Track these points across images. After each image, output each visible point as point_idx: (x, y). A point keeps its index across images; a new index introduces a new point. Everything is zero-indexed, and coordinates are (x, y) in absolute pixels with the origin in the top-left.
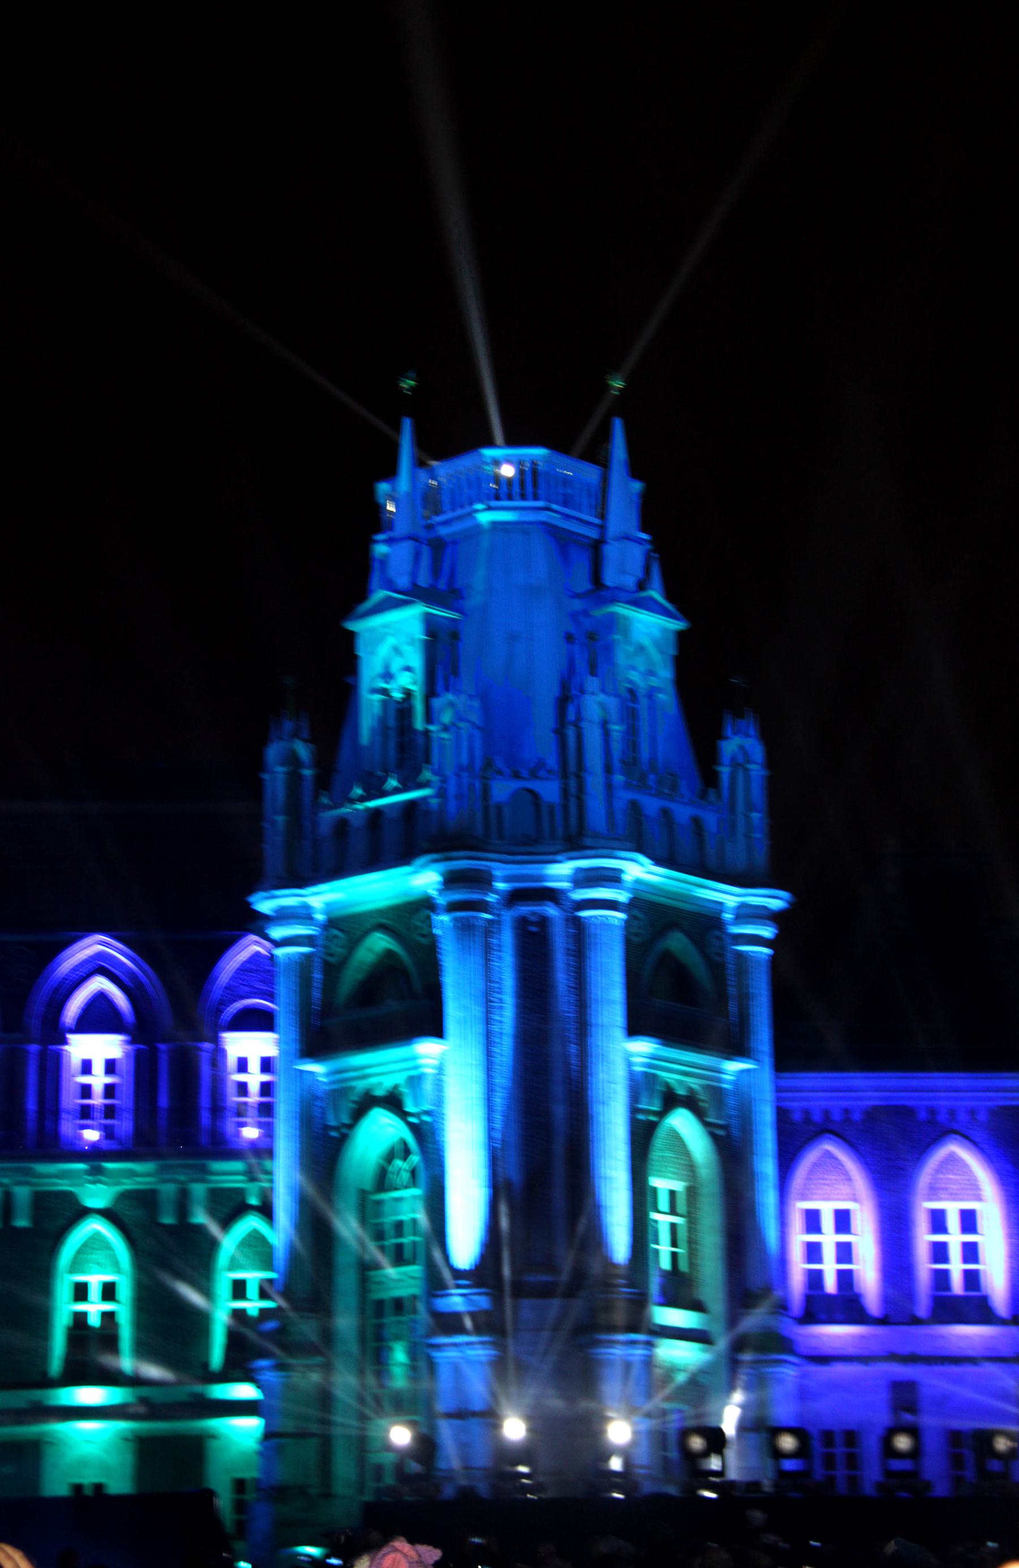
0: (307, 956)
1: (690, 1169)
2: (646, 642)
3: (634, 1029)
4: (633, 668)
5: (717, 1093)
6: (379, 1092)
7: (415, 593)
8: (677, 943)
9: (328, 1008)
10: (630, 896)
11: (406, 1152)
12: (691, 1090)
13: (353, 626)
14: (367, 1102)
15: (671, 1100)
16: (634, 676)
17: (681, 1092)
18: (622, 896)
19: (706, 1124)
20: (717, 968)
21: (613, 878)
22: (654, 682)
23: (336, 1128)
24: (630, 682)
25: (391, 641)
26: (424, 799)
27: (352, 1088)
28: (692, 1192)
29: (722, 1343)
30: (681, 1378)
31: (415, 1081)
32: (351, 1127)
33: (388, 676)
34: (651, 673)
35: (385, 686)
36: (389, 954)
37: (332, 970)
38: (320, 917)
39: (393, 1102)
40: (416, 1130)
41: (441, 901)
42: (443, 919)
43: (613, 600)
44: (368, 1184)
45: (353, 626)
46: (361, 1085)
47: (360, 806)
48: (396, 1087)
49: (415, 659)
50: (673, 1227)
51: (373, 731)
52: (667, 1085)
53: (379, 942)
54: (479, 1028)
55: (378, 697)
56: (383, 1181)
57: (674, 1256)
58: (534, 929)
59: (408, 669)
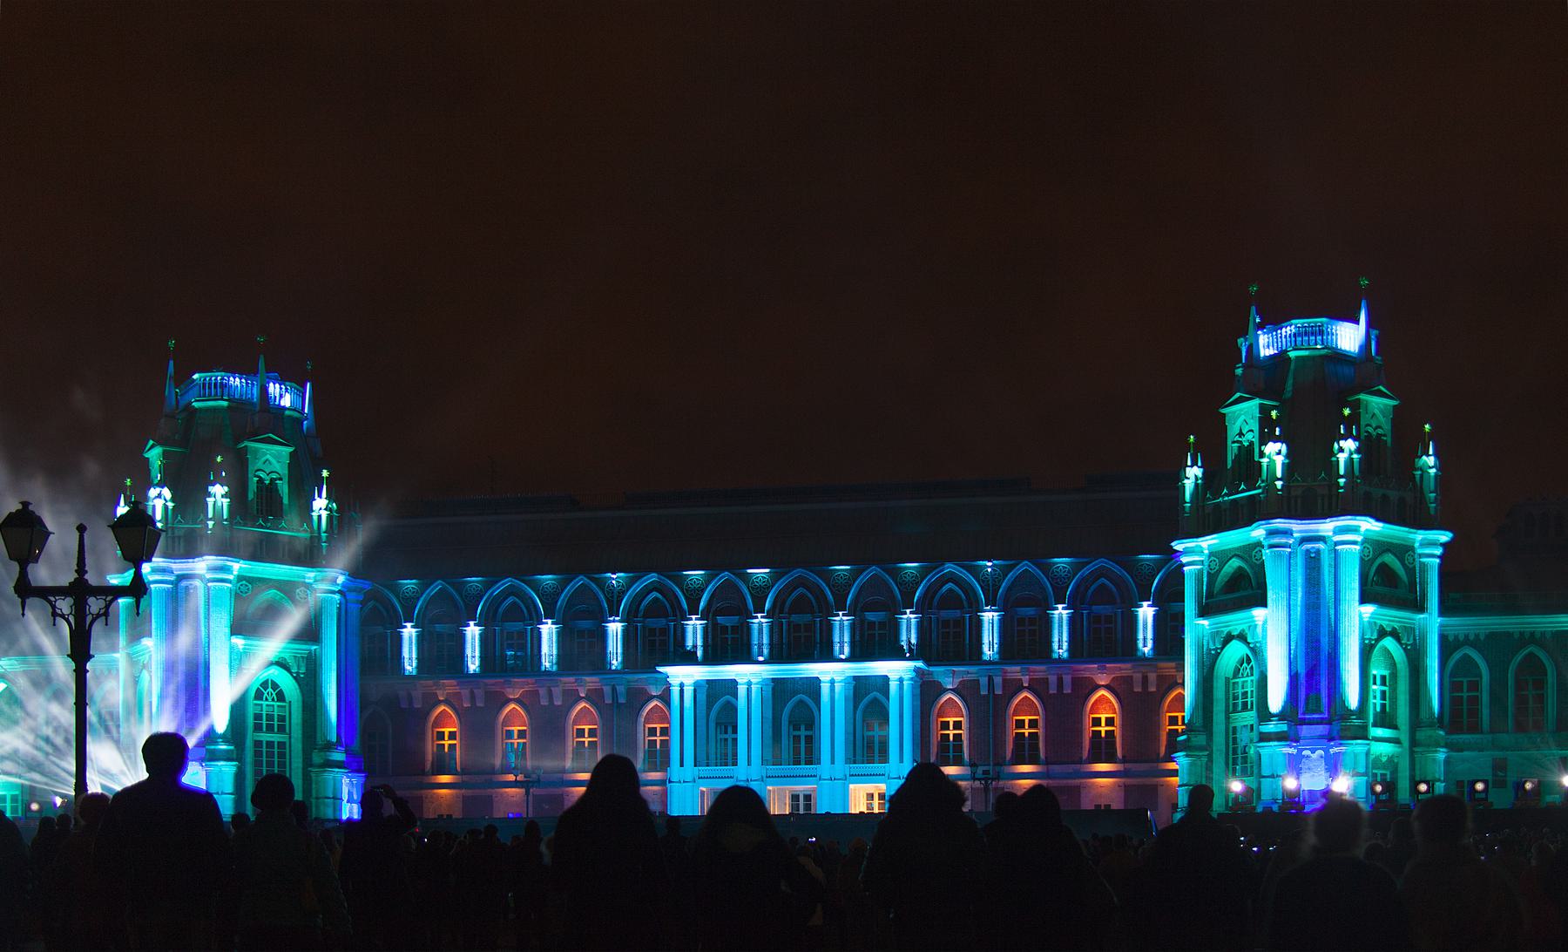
0: (1201, 572)
1: (1392, 665)
2: (1377, 411)
3: (1364, 600)
4: (1368, 425)
5: (1410, 630)
6: (1235, 633)
7: (1255, 394)
8: (1389, 559)
9: (1210, 594)
10: (1362, 537)
11: (1249, 661)
12: (1394, 629)
13: (1223, 411)
14: (1229, 638)
15: (1382, 633)
16: (1370, 429)
17: (1389, 629)
18: (1359, 539)
19: (1401, 644)
20: (1411, 571)
21: (1355, 530)
22: (1380, 431)
23: (1213, 649)
24: (1367, 432)
25: (1242, 418)
26: (1259, 494)
27: (1222, 631)
28: (1394, 675)
29: (1406, 744)
30: (1384, 759)
31: (1253, 627)
32: (1222, 649)
33: (1241, 434)
34: (1378, 427)
35: (1240, 439)
36: (1240, 568)
37: (1212, 577)
38: (1206, 552)
39: (1242, 637)
40: (1253, 650)
41: (1265, 543)
42: (1266, 553)
43: (1358, 392)
44: (1230, 675)
45: (1223, 411)
46: (1226, 630)
47: (1226, 498)
48: (1243, 630)
49: (1256, 428)
50: (1383, 693)
51: (1233, 462)
52: (1381, 626)
53: (1235, 563)
54: (1285, 603)
55: (1236, 445)
56: (1236, 672)
57: (1383, 706)
58: (1313, 555)
59: (1252, 431)
